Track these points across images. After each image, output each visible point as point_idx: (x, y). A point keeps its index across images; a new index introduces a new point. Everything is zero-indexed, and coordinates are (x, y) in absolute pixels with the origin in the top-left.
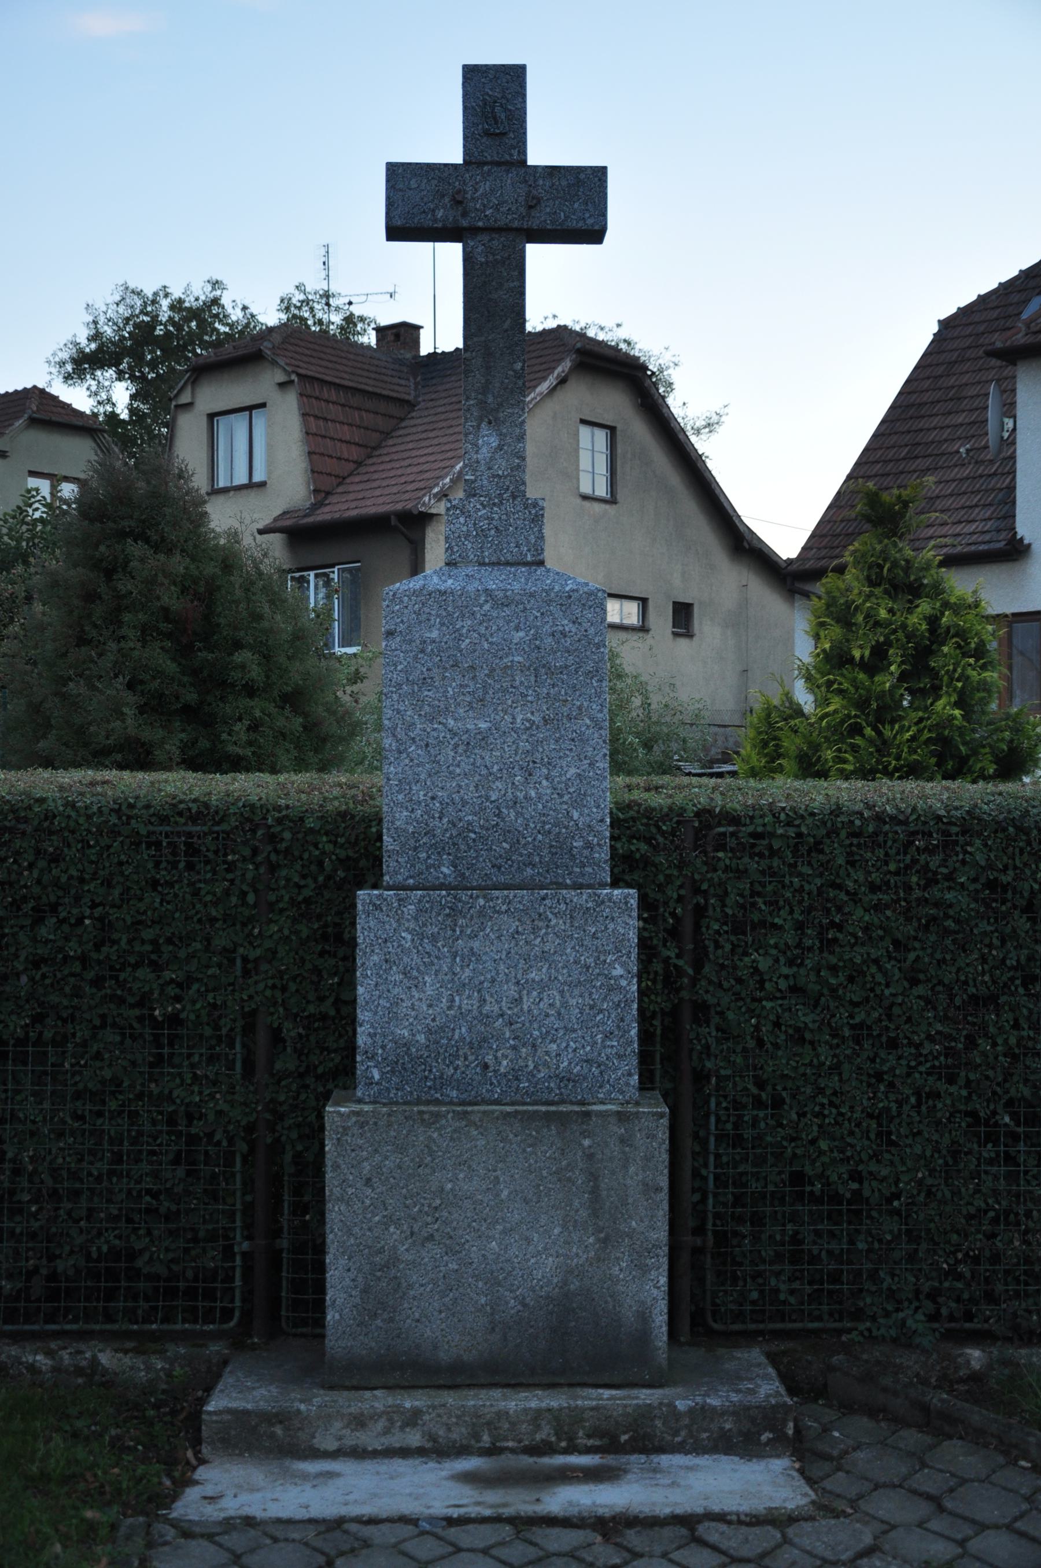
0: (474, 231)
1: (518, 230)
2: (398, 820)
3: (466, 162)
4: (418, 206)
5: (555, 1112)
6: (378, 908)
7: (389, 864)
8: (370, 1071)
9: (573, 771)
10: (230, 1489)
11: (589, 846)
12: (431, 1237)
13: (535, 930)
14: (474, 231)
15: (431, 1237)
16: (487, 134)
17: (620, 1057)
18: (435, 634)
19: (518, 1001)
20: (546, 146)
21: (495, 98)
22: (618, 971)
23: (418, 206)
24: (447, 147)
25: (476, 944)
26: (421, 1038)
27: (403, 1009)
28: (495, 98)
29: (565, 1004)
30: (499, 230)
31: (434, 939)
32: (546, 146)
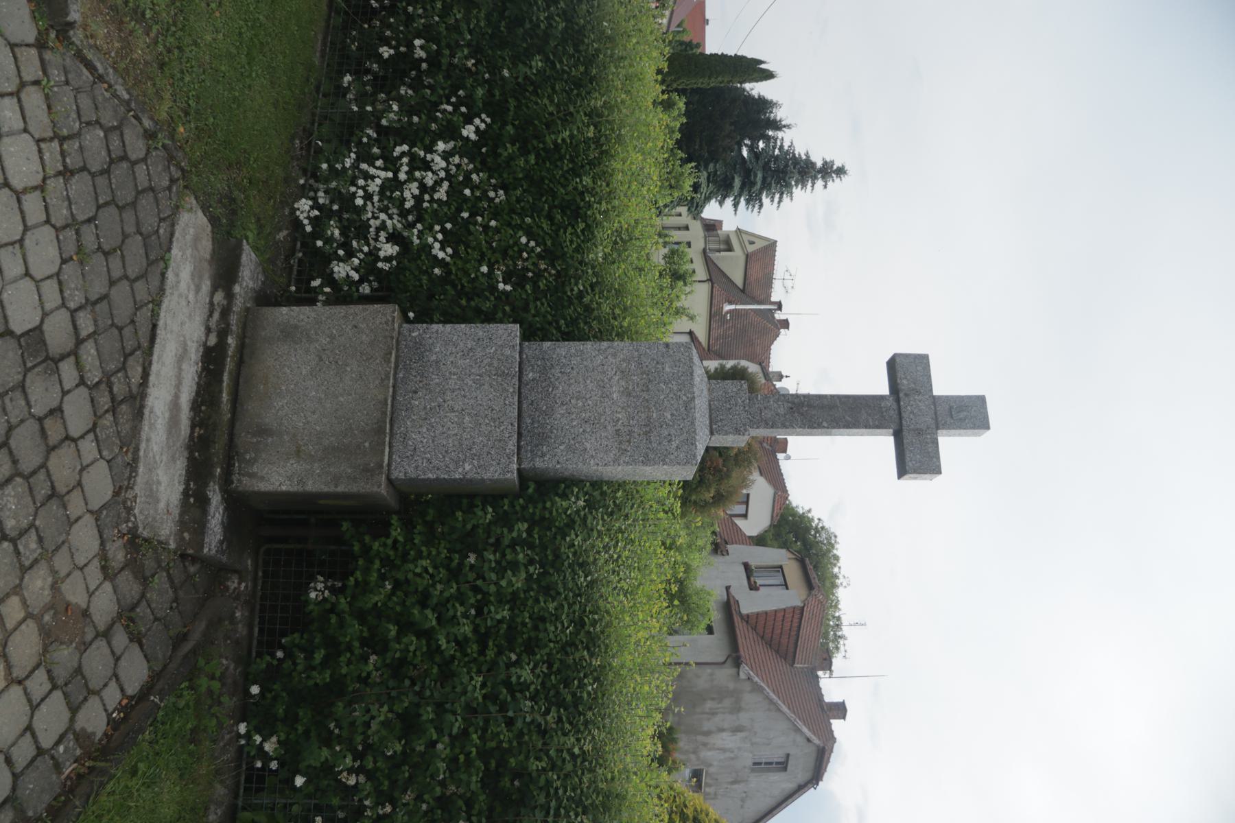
0: (898, 401)
1: (901, 424)
2: (563, 349)
3: (936, 400)
4: (907, 372)
5: (385, 426)
6: (509, 335)
7: (534, 345)
8: (418, 330)
9: (588, 446)
10: (192, 232)
11: (543, 455)
12: (321, 359)
13: (494, 420)
14: (898, 401)
15: (321, 359)
16: (951, 408)
17: (417, 467)
18: (667, 369)
19: (452, 410)
20: (950, 445)
21: (969, 414)
22: (467, 467)
23: (907, 372)
24: (943, 385)
25: (486, 387)
26: (434, 357)
27: (451, 348)
28: (969, 414)
29: (448, 437)
30: (900, 414)
31: (490, 365)
32: (950, 445)
